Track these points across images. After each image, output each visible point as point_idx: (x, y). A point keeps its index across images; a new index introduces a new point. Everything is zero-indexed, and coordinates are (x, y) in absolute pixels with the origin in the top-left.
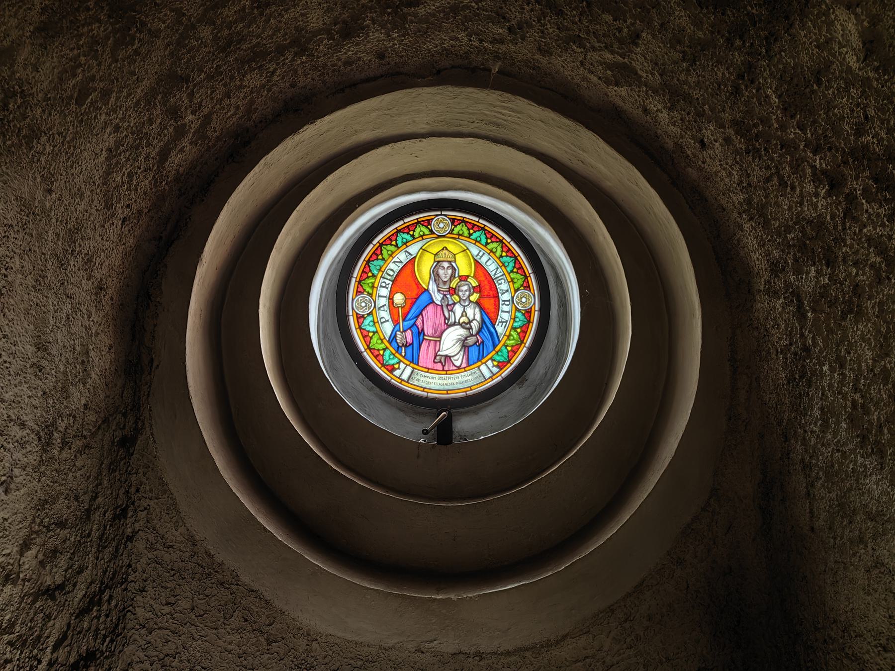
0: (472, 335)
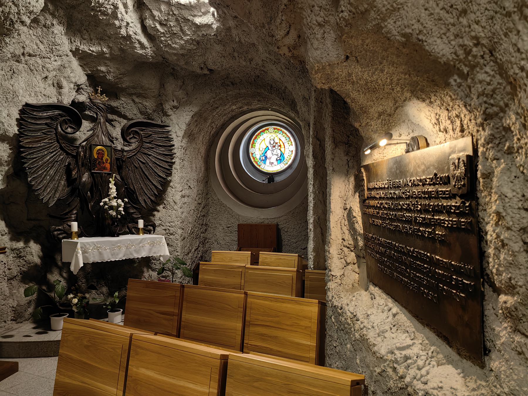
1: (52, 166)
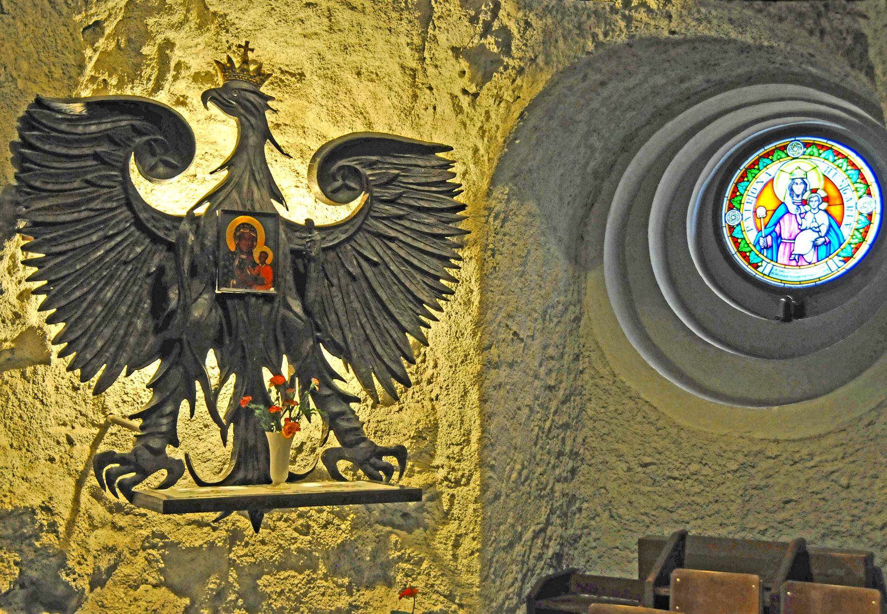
0: (821, 237)
1: (112, 277)
